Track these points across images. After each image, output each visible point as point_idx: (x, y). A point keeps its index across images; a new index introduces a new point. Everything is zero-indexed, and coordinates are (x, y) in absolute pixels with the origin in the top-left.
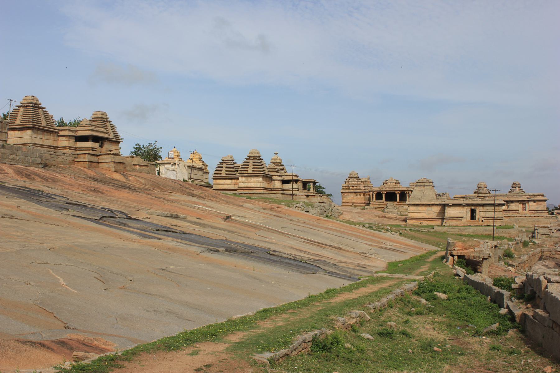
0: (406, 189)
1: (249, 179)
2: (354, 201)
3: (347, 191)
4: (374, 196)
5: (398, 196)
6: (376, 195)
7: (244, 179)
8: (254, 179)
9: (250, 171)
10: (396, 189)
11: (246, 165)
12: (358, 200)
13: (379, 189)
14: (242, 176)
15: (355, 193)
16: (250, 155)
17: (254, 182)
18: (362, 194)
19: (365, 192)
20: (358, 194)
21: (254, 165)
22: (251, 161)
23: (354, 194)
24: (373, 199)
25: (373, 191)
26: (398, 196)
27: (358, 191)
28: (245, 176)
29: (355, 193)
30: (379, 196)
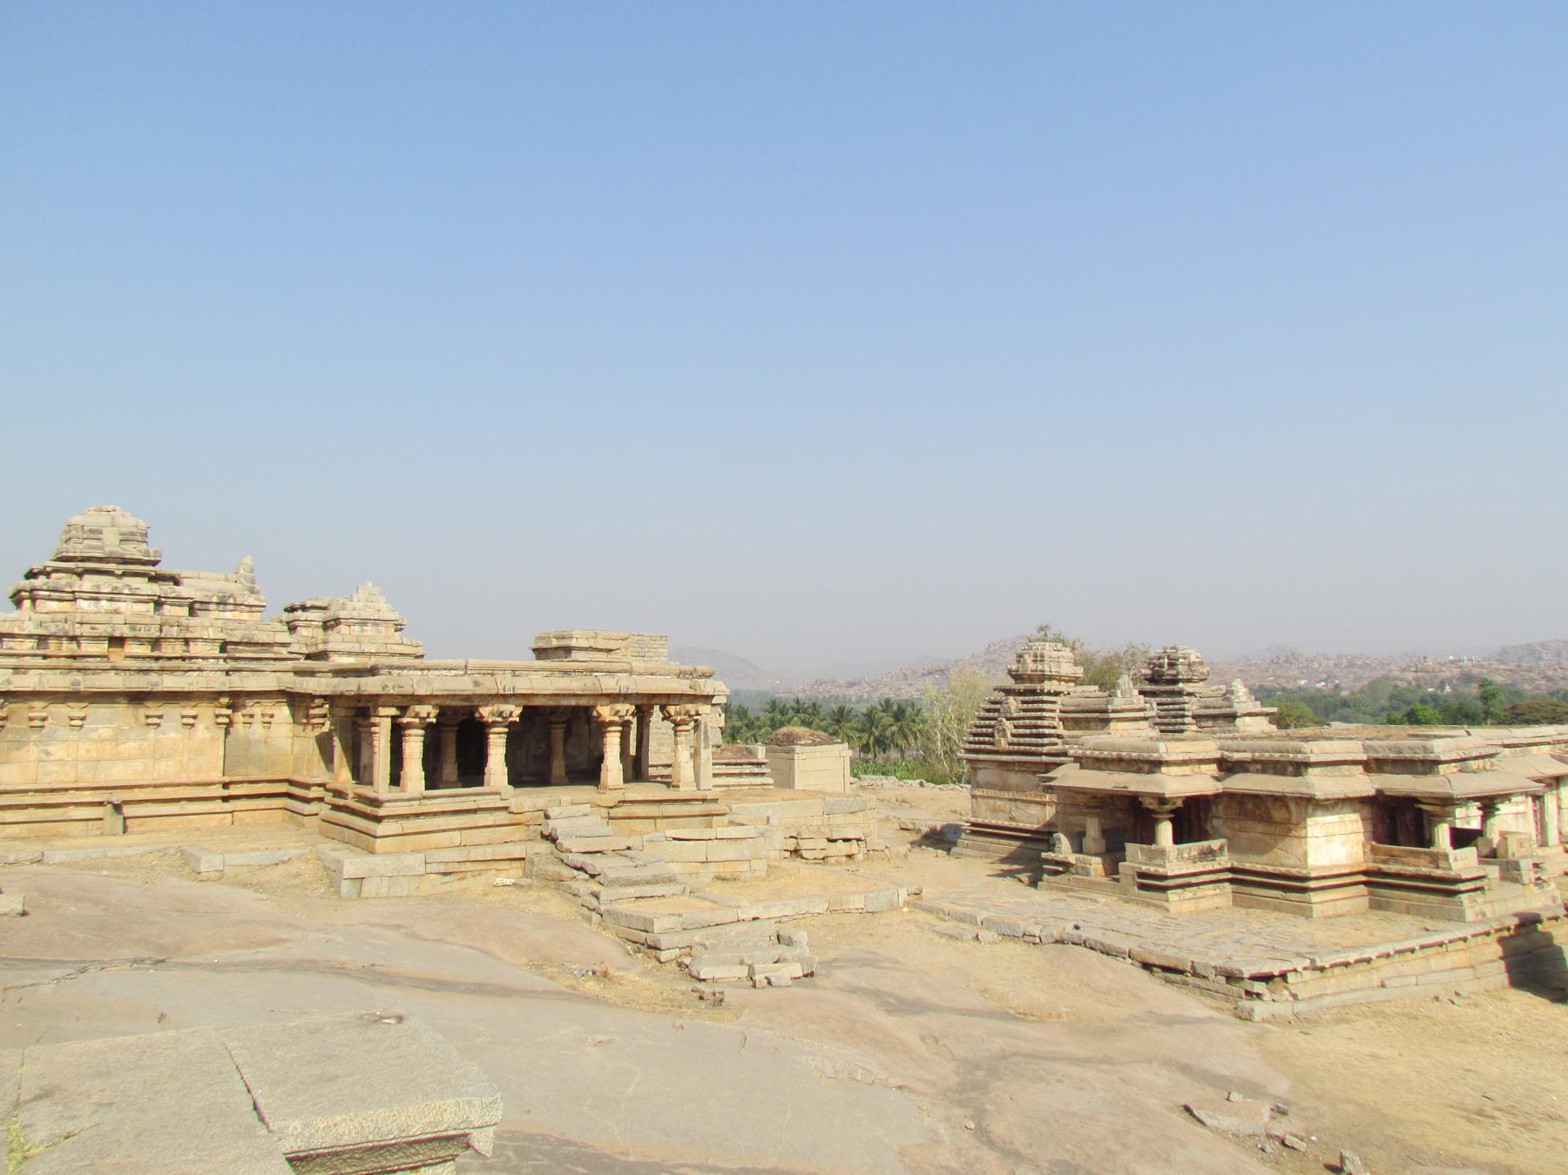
0: (682, 686)
2: (120, 773)
3: (60, 682)
4: (414, 746)
12: (166, 770)
13: (464, 685)
15: (137, 698)
18: (206, 711)
19: (237, 699)
20: (172, 712)
23: (122, 709)
24: (395, 780)
25: (405, 702)
26: (612, 743)
27: (170, 683)
29: (137, 698)
30: (457, 743)
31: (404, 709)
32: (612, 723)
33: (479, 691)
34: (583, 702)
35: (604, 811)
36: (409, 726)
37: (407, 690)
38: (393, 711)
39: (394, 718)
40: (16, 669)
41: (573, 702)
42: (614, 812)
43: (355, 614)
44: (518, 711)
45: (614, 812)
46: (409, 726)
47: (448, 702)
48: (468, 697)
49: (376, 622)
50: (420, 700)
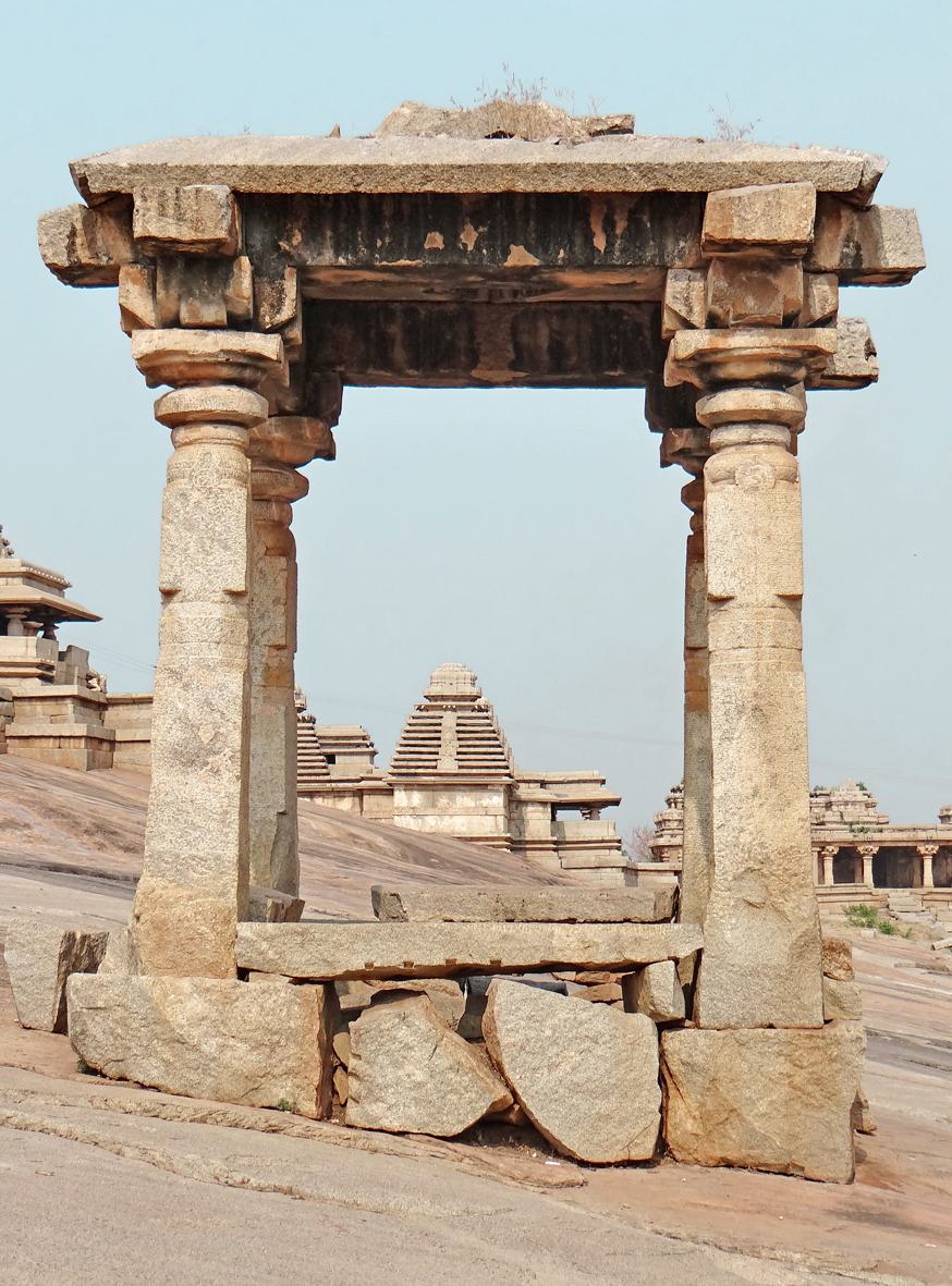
1: (443, 799)
4: (829, 864)
5: (928, 863)
6: (836, 859)
7: (417, 798)
8: (464, 800)
9: (448, 764)
10: (922, 835)
11: (421, 738)
14: (409, 787)
16: (436, 690)
17: (467, 812)
21: (462, 733)
22: (449, 720)
26: (928, 863)
28: (423, 787)
31: (823, 848)
32: (926, 855)
33: (857, 839)
34: (910, 844)
35: (920, 897)
36: (825, 856)
37: (823, 839)
38: (818, 849)
39: (819, 852)
40: (672, 836)
41: (905, 844)
42: (925, 897)
43: (840, 799)
44: (877, 849)
45: (925, 897)
46: (825, 856)
47: (842, 845)
48: (852, 842)
49: (854, 803)
50: (829, 843)
